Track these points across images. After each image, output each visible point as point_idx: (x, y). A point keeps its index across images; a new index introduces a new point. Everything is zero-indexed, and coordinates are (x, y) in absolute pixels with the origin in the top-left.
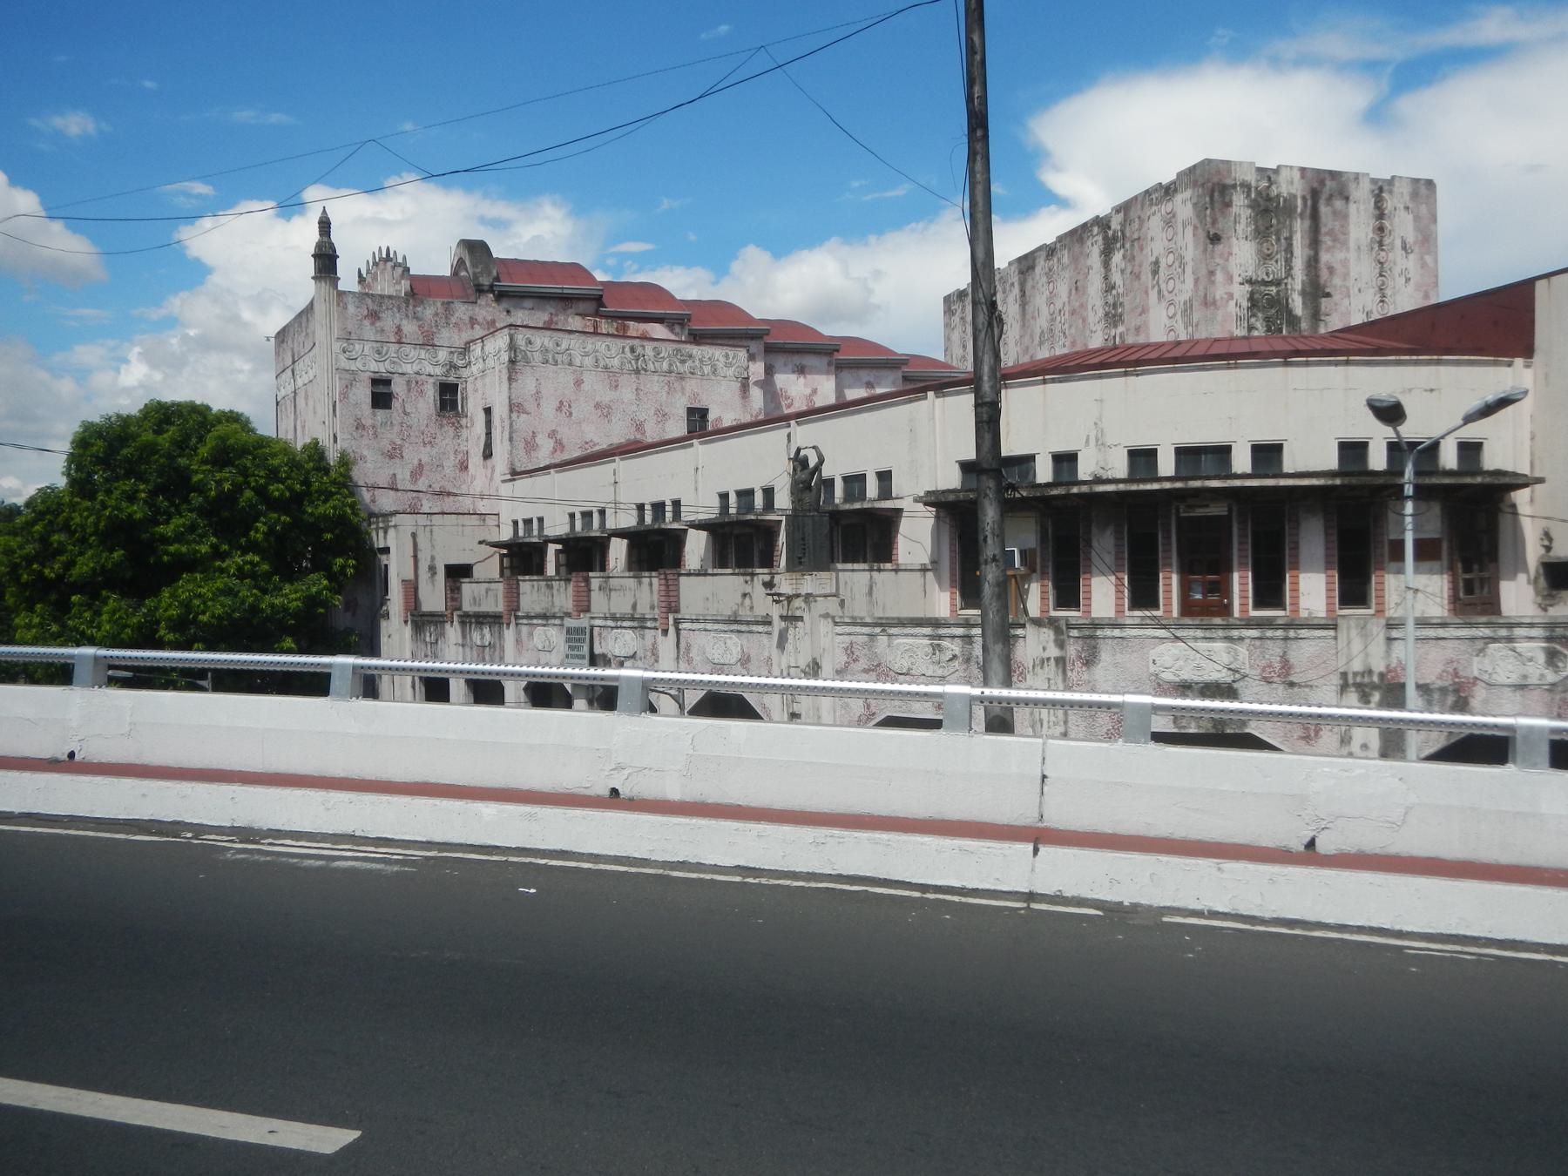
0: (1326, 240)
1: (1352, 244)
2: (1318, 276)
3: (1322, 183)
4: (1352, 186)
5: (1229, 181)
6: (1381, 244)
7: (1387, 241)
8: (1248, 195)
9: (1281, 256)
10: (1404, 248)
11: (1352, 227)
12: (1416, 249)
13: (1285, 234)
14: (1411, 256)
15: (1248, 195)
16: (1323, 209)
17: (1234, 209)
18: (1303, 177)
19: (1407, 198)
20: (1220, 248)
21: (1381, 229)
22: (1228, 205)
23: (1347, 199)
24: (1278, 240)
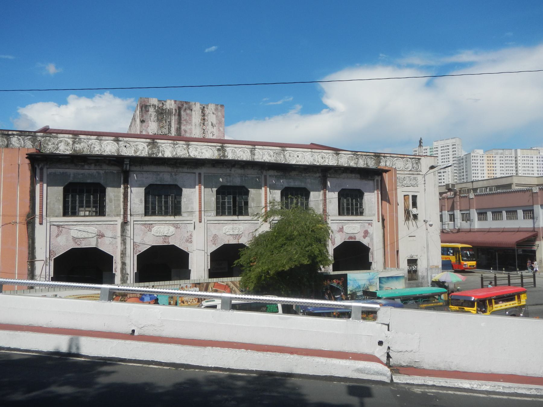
0: (184, 122)
1: (193, 124)
2: (180, 133)
3: (183, 105)
4: (193, 106)
5: (148, 104)
6: (204, 124)
7: (206, 123)
8: (155, 108)
9: (167, 127)
10: (212, 125)
11: (193, 118)
12: (217, 125)
13: (169, 120)
14: (215, 128)
15: (155, 108)
16: (182, 113)
17: (150, 113)
18: (175, 103)
19: (213, 110)
20: (144, 124)
21: (204, 119)
22: (148, 111)
23: (192, 110)
24: (166, 122)
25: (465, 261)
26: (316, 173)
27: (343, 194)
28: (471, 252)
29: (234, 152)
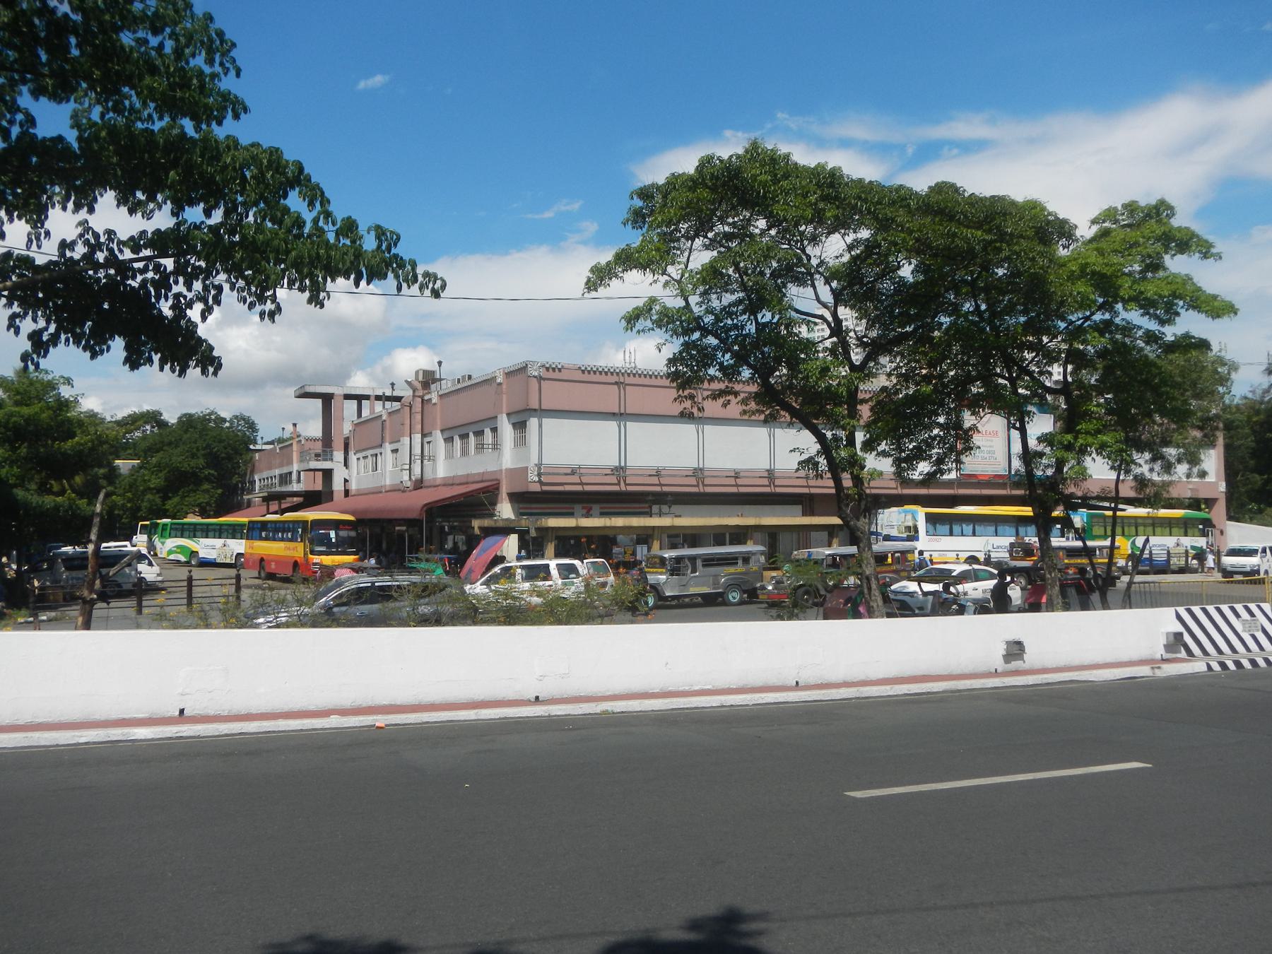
25: (321, 553)
28: (343, 533)
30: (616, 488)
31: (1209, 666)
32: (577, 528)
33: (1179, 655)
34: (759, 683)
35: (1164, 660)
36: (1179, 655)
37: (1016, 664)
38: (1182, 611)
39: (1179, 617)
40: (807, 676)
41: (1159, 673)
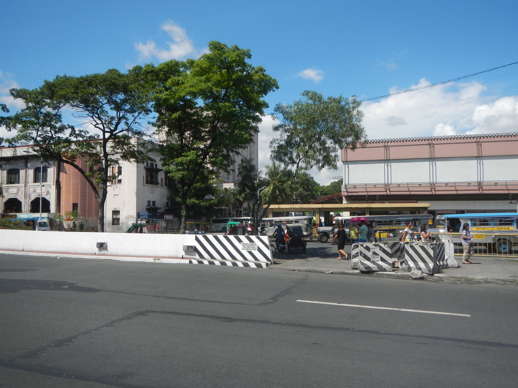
26: (22, 160)
27: (37, 171)
29: (20, 152)
30: (385, 193)
31: (191, 262)
32: (279, 208)
33: (194, 257)
34: (12, 248)
35: (183, 258)
36: (194, 257)
37: (103, 252)
38: (200, 237)
39: (197, 239)
40: (27, 248)
41: (157, 261)
